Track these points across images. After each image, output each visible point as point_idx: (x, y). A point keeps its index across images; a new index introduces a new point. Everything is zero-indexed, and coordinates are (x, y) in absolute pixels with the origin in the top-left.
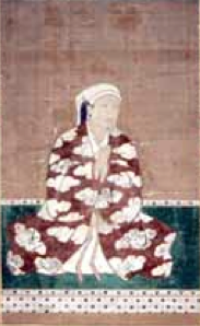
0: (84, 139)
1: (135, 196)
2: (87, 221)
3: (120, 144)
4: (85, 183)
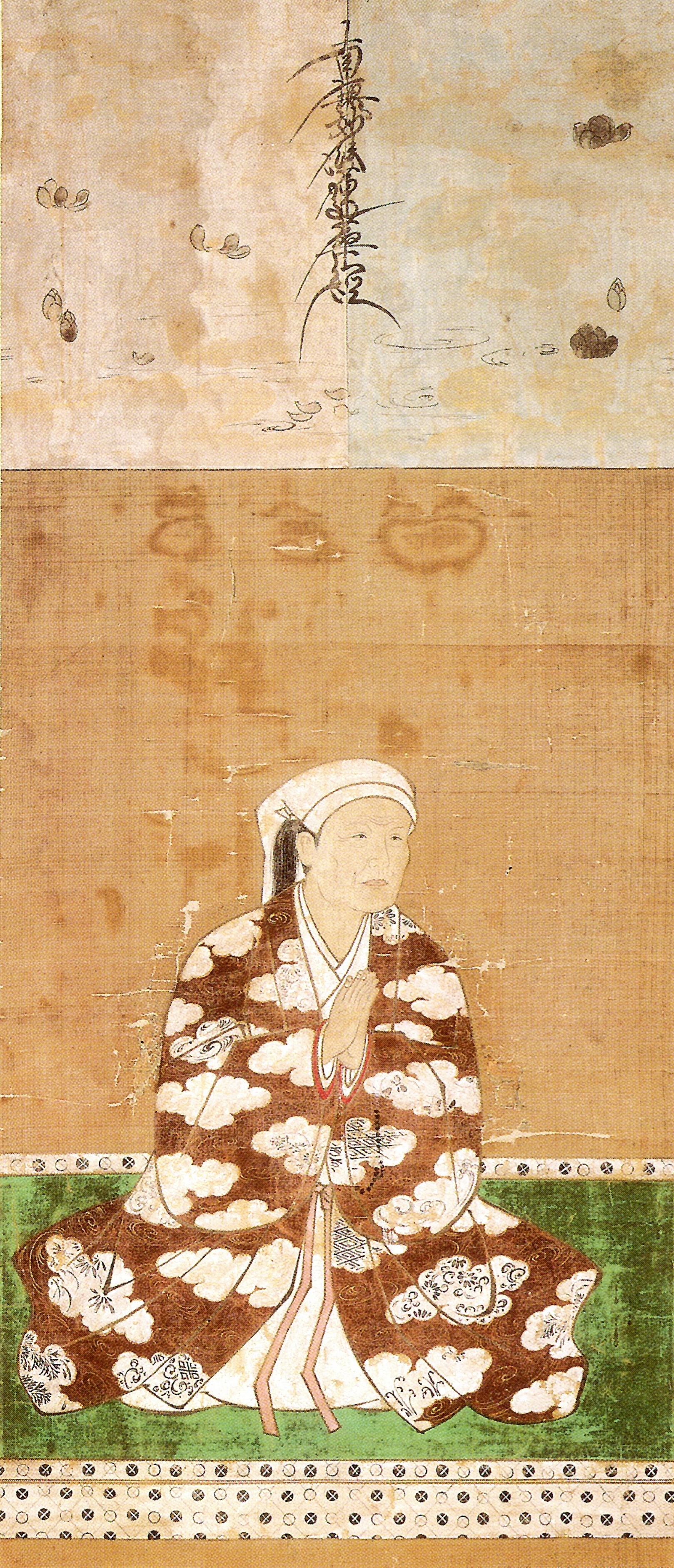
0: (286, 950)
1: (458, 1144)
2: (294, 1228)
3: (411, 967)
4: (287, 1098)
